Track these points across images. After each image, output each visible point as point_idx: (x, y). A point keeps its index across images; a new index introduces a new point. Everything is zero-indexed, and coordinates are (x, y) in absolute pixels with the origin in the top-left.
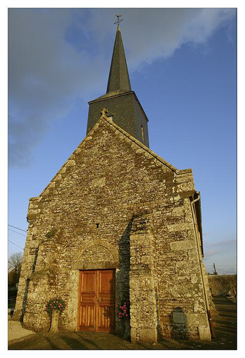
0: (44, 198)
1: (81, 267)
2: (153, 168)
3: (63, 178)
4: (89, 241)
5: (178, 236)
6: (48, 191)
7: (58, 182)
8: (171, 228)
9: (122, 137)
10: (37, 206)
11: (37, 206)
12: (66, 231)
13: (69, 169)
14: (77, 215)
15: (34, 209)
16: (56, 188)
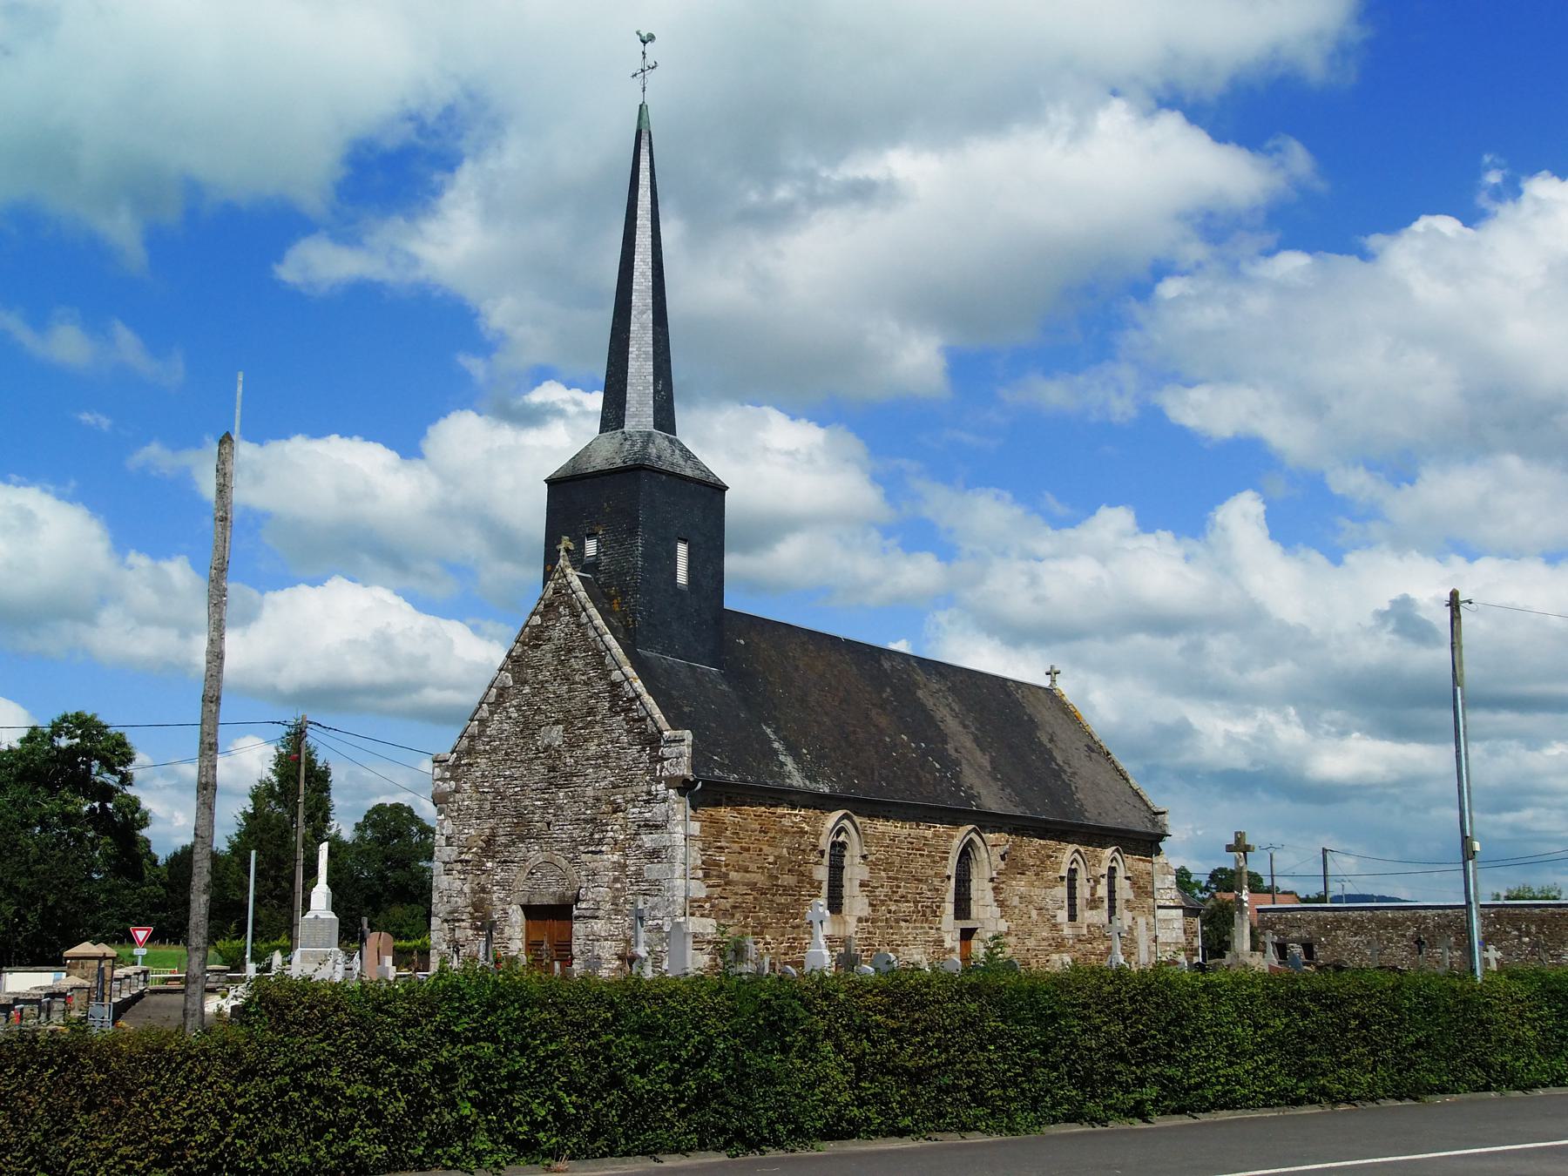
0: (459, 758)
1: (524, 901)
2: (635, 720)
3: (492, 713)
4: (536, 855)
5: (654, 855)
6: (465, 742)
7: (482, 722)
8: (648, 841)
9: (592, 633)
10: (448, 775)
11: (448, 775)
12: (501, 831)
13: (503, 692)
14: (516, 801)
15: (443, 780)
16: (480, 736)
